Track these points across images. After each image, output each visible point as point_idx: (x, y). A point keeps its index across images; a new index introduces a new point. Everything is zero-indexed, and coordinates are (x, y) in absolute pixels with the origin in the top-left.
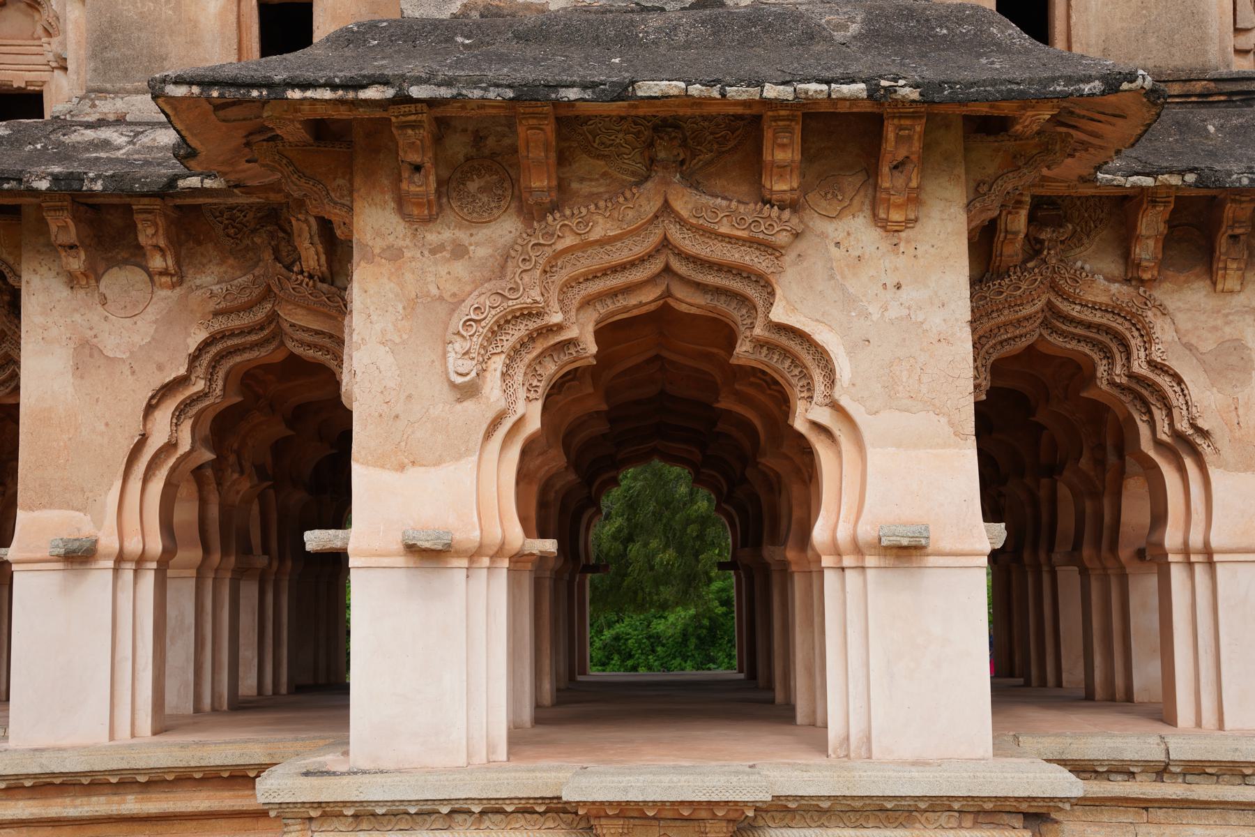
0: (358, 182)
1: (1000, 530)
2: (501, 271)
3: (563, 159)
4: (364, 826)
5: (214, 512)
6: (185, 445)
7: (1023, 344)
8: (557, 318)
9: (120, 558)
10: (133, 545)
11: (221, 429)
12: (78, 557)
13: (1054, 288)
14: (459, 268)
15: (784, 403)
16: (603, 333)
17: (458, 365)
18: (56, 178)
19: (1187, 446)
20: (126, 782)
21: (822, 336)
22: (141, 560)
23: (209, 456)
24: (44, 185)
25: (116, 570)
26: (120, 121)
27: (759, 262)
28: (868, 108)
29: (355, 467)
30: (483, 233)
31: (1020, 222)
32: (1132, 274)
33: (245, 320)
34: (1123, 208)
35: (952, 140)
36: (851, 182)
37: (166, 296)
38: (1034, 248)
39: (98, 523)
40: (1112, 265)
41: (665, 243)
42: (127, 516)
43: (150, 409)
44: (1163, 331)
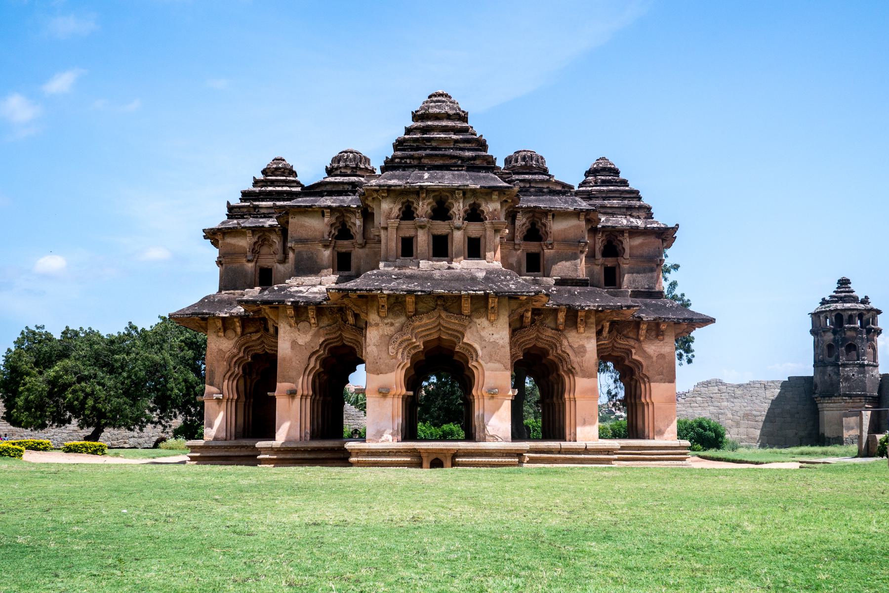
1: (516, 391)
2: (401, 330)
3: (416, 304)
5: (317, 384)
6: (318, 367)
7: (530, 346)
8: (414, 340)
10: (306, 393)
11: (324, 362)
12: (292, 394)
13: (538, 331)
14: (392, 328)
15: (467, 362)
16: (425, 343)
18: (292, 302)
19: (571, 372)
20: (305, 451)
22: (307, 396)
23: (322, 370)
26: (302, 285)
27: (461, 329)
31: (529, 314)
32: (557, 329)
33: (334, 336)
34: (555, 312)
35: (505, 301)
36: (482, 310)
37: (314, 329)
38: (533, 321)
40: (553, 325)
41: (439, 324)
42: (303, 384)
43: (310, 358)
44: (565, 343)
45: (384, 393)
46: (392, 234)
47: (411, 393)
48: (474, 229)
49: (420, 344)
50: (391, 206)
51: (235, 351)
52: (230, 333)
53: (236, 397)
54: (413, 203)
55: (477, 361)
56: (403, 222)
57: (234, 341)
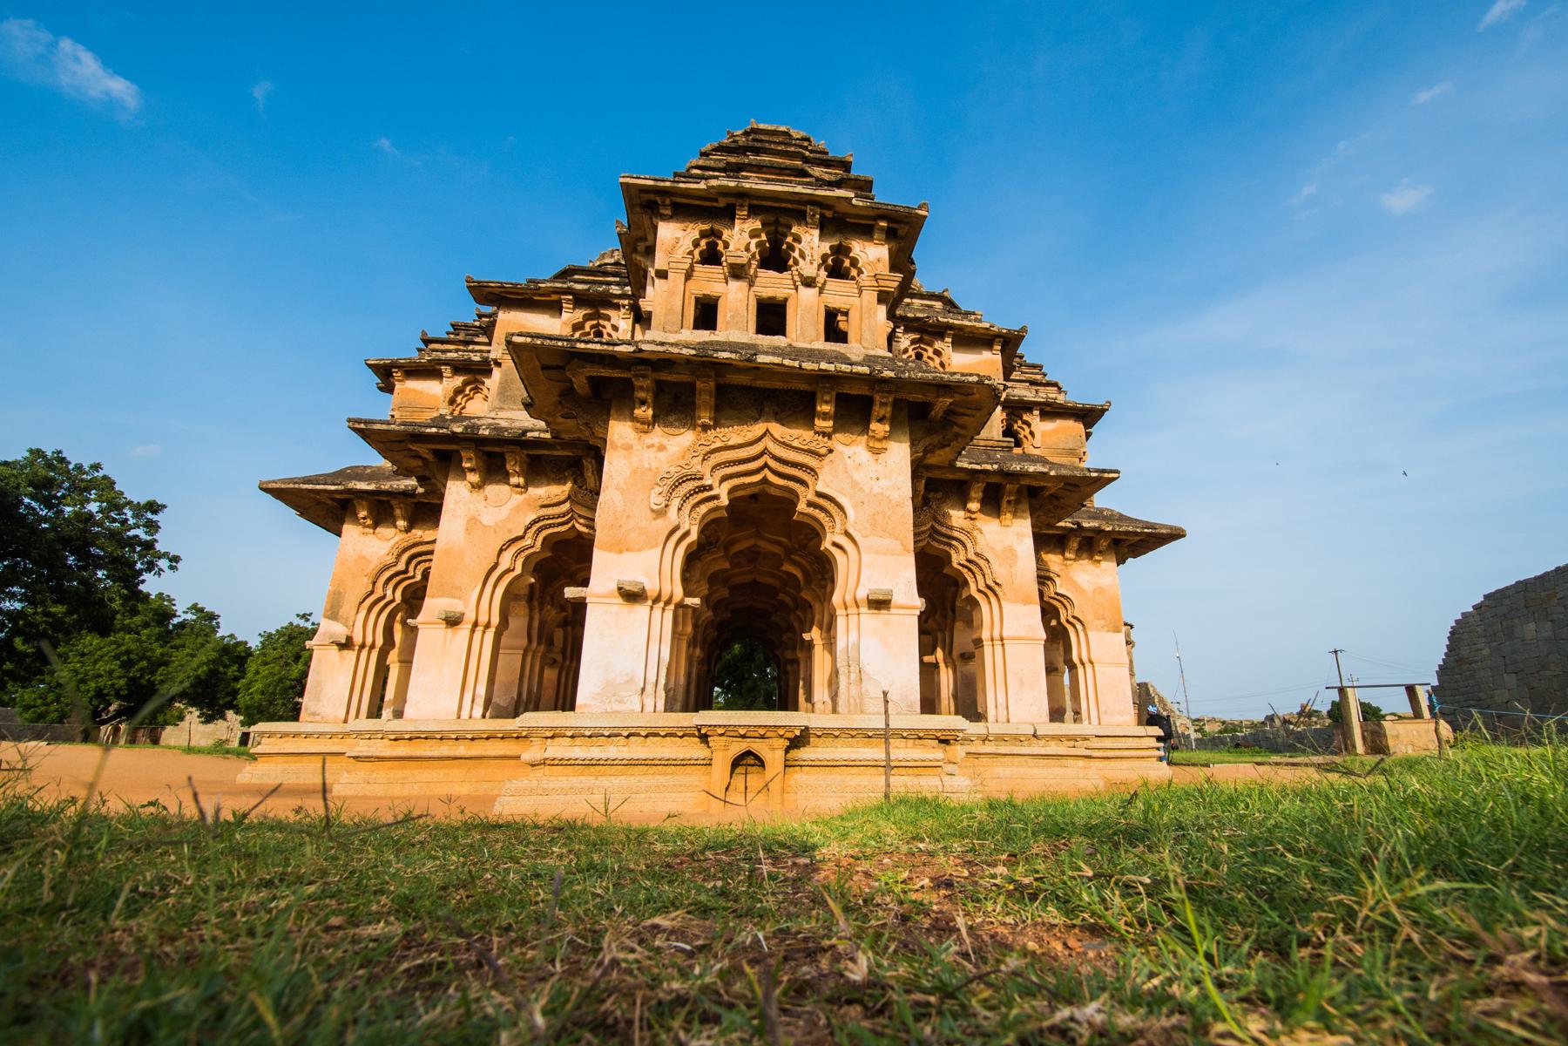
0: (613, 412)
4: (578, 741)
6: (518, 571)
9: (476, 624)
12: (453, 622)
14: (661, 455)
16: (730, 492)
17: (656, 500)
21: (841, 499)
24: (459, 430)
25: (473, 631)
28: (864, 391)
29: (596, 551)
30: (676, 439)
39: (466, 606)
43: (501, 551)
45: (632, 596)
46: (676, 278)
47: (695, 601)
48: (838, 293)
49: (723, 492)
50: (680, 234)
51: (390, 560)
52: (385, 531)
53: (380, 642)
54: (719, 235)
55: (847, 534)
56: (698, 267)
57: (392, 542)
